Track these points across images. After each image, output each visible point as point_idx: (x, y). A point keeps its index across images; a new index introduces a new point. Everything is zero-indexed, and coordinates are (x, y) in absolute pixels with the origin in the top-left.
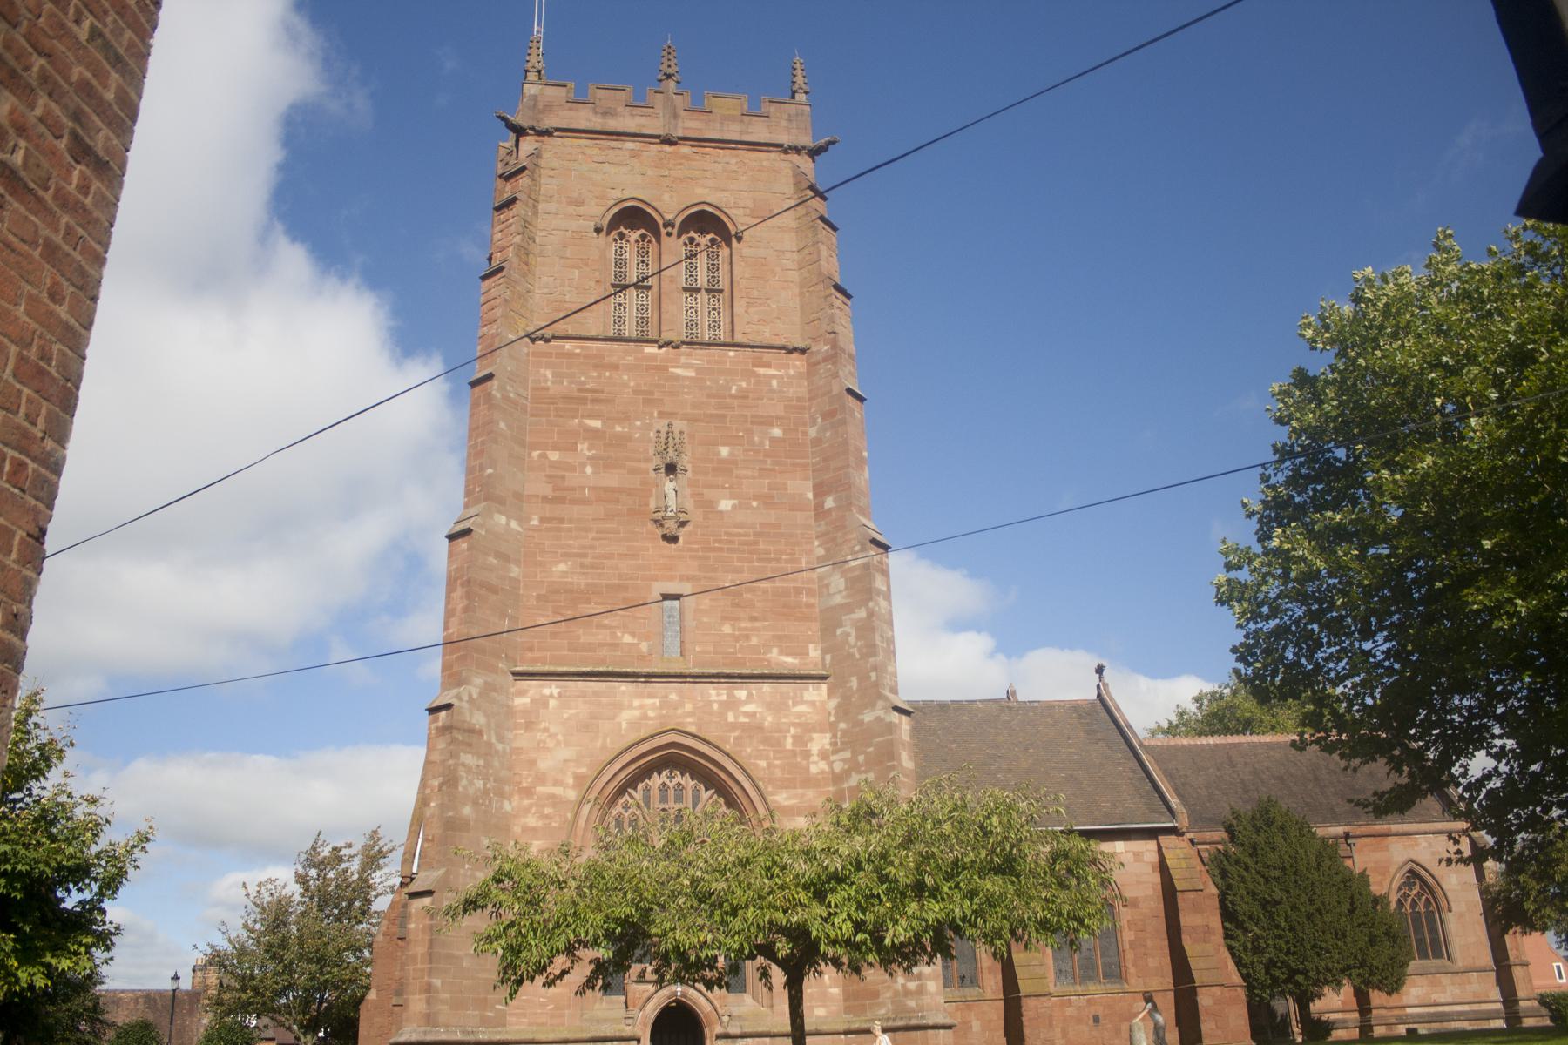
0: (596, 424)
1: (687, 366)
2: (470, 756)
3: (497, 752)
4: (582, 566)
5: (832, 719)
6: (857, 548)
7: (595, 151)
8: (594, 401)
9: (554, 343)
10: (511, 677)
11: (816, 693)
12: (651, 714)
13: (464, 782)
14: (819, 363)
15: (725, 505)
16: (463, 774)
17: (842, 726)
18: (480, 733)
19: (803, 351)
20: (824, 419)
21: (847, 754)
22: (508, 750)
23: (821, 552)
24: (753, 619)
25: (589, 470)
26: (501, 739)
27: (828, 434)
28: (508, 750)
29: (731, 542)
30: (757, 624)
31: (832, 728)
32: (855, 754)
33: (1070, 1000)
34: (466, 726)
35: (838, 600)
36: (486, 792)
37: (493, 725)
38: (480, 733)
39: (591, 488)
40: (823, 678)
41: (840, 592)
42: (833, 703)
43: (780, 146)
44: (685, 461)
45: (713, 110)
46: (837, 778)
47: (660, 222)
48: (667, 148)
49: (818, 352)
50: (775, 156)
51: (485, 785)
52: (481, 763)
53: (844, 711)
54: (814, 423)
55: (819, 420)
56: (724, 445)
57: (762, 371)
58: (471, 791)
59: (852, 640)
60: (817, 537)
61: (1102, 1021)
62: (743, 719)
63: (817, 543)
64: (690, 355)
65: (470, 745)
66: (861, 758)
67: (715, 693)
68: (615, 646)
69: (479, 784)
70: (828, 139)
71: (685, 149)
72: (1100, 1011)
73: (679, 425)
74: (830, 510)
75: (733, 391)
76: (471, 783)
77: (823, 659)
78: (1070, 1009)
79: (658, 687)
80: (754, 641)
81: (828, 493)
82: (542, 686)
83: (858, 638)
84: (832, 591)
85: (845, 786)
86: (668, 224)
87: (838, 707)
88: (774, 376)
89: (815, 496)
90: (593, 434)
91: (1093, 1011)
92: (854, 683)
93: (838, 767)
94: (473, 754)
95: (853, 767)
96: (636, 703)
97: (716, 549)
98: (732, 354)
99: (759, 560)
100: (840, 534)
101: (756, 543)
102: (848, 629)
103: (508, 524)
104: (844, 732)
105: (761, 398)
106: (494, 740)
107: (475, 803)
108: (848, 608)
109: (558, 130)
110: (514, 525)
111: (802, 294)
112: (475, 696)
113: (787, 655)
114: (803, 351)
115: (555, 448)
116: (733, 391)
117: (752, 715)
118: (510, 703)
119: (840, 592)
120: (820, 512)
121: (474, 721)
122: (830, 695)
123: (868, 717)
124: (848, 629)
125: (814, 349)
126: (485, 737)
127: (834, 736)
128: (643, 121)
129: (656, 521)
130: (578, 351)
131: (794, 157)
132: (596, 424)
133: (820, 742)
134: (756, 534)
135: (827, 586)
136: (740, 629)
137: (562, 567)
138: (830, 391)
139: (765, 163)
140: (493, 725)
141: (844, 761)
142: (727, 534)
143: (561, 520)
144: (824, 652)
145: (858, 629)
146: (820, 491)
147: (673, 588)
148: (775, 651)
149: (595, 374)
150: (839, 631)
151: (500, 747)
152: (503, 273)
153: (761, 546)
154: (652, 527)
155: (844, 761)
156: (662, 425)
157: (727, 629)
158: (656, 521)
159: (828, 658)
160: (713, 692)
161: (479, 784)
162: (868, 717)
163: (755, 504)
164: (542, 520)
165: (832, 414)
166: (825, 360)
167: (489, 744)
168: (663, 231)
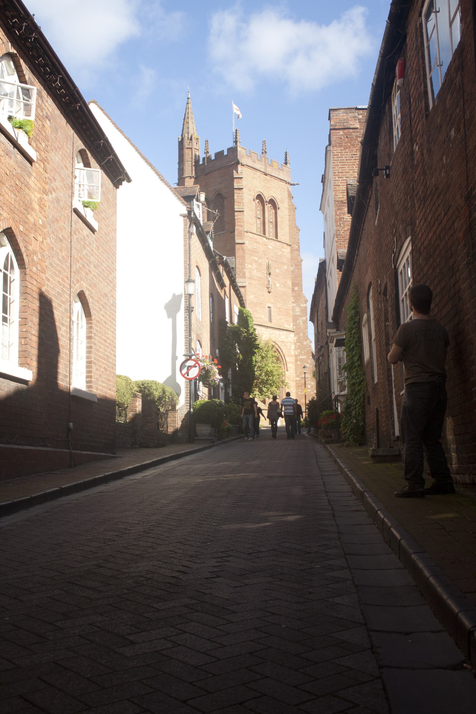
0: (256, 258)
1: (271, 246)
4: (256, 297)
5: (295, 342)
6: (304, 302)
7: (252, 174)
8: (256, 252)
9: (248, 233)
11: (292, 335)
12: (268, 336)
14: (294, 250)
15: (278, 285)
17: (298, 344)
19: (290, 246)
20: (295, 266)
21: (299, 351)
23: (294, 301)
24: (282, 315)
25: (255, 271)
27: (296, 271)
29: (279, 295)
30: (283, 317)
31: (295, 344)
32: (301, 351)
35: (298, 314)
39: (256, 276)
40: (294, 332)
41: (298, 312)
42: (296, 338)
43: (286, 181)
44: (272, 274)
45: (274, 166)
46: (296, 356)
47: (265, 201)
48: (265, 176)
49: (294, 247)
50: (283, 184)
53: (298, 341)
54: (292, 266)
55: (294, 266)
56: (277, 269)
57: (283, 250)
59: (301, 324)
60: (292, 296)
62: (282, 340)
63: (292, 298)
64: (271, 242)
66: (303, 352)
67: (277, 332)
68: (261, 318)
70: (297, 183)
71: (268, 177)
73: (270, 262)
74: (296, 291)
75: (279, 254)
77: (293, 327)
79: (269, 330)
80: (283, 321)
81: (296, 286)
83: (303, 324)
84: (296, 311)
85: (298, 358)
86: (266, 202)
87: (297, 339)
88: (285, 252)
89: (292, 286)
90: (256, 261)
92: (302, 335)
93: (296, 353)
95: (301, 354)
96: (265, 333)
97: (277, 297)
98: (278, 244)
99: (283, 301)
100: (299, 297)
101: (282, 296)
102: (300, 321)
104: (298, 346)
105: (283, 257)
108: (301, 316)
109: (246, 165)
111: (290, 229)
113: (288, 325)
114: (290, 246)
115: (250, 264)
116: (279, 254)
117: (283, 339)
119: (298, 312)
120: (293, 290)
122: (295, 336)
123: (305, 343)
124: (300, 321)
125: (293, 246)
127: (296, 346)
128: (261, 166)
129: (267, 288)
130: (252, 237)
131: (287, 185)
132: (256, 258)
133: (293, 347)
134: (283, 294)
135: (295, 309)
137: (252, 296)
138: (298, 259)
139: (283, 186)
141: (298, 352)
142: (278, 293)
143: (251, 284)
144: (294, 325)
145: (303, 322)
146: (294, 285)
148: (286, 324)
149: (255, 244)
150: (298, 321)
152: (243, 213)
153: (283, 297)
154: (266, 289)
155: (298, 352)
156: (267, 261)
157: (278, 317)
158: (267, 288)
159: (295, 327)
162: (305, 343)
163: (282, 286)
164: (249, 283)
165: (298, 265)
166: (297, 250)
168: (265, 203)
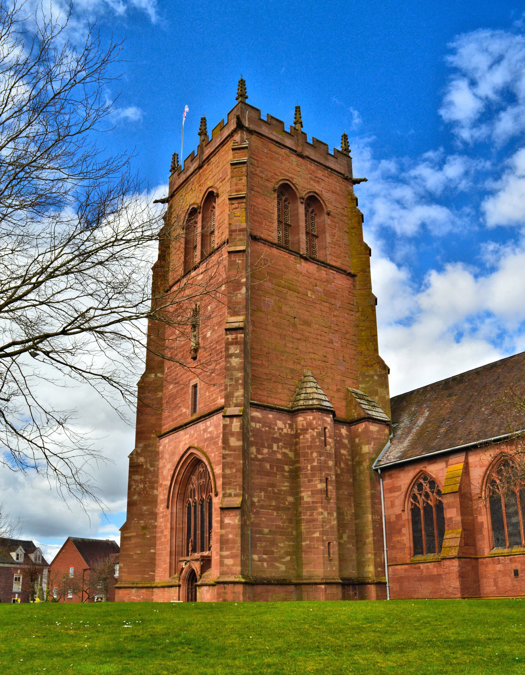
2: (137, 476)
3: (150, 471)
10: (158, 439)
13: (134, 487)
16: (133, 484)
18: (142, 465)
22: (156, 469)
26: (151, 466)
28: (156, 469)
33: (499, 559)
34: (135, 464)
36: (145, 488)
37: (148, 461)
38: (142, 465)
51: (144, 486)
52: (143, 477)
58: (138, 489)
61: (520, 575)
65: (137, 472)
69: (142, 486)
72: (518, 567)
76: (137, 486)
78: (499, 565)
82: (165, 440)
91: (514, 566)
94: (138, 475)
103: (156, 376)
106: (149, 466)
107: (139, 494)
110: (159, 375)
112: (139, 451)
118: (157, 450)
121: (139, 461)
126: (145, 467)
136: (211, 392)
140: (148, 461)
147: (193, 383)
151: (152, 469)
160: (201, 426)
161: (142, 486)
167: (147, 469)
